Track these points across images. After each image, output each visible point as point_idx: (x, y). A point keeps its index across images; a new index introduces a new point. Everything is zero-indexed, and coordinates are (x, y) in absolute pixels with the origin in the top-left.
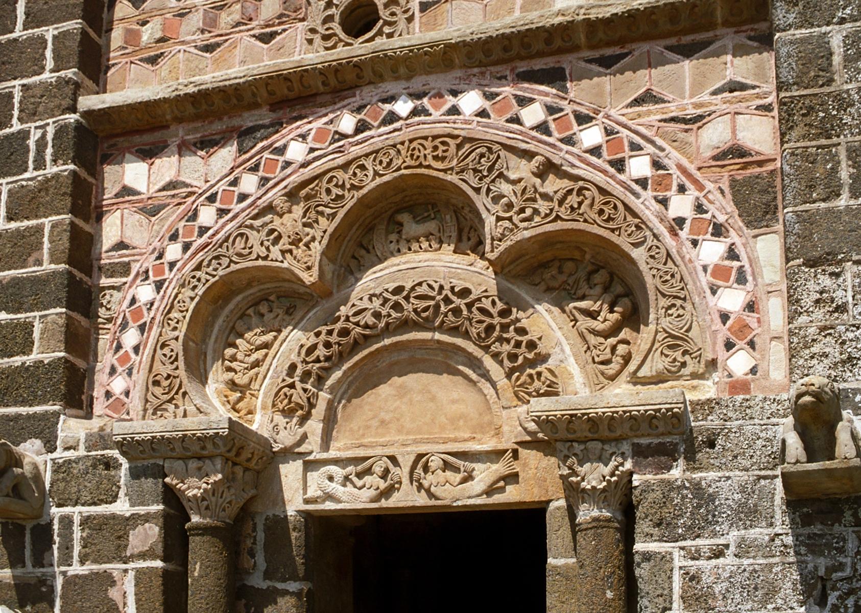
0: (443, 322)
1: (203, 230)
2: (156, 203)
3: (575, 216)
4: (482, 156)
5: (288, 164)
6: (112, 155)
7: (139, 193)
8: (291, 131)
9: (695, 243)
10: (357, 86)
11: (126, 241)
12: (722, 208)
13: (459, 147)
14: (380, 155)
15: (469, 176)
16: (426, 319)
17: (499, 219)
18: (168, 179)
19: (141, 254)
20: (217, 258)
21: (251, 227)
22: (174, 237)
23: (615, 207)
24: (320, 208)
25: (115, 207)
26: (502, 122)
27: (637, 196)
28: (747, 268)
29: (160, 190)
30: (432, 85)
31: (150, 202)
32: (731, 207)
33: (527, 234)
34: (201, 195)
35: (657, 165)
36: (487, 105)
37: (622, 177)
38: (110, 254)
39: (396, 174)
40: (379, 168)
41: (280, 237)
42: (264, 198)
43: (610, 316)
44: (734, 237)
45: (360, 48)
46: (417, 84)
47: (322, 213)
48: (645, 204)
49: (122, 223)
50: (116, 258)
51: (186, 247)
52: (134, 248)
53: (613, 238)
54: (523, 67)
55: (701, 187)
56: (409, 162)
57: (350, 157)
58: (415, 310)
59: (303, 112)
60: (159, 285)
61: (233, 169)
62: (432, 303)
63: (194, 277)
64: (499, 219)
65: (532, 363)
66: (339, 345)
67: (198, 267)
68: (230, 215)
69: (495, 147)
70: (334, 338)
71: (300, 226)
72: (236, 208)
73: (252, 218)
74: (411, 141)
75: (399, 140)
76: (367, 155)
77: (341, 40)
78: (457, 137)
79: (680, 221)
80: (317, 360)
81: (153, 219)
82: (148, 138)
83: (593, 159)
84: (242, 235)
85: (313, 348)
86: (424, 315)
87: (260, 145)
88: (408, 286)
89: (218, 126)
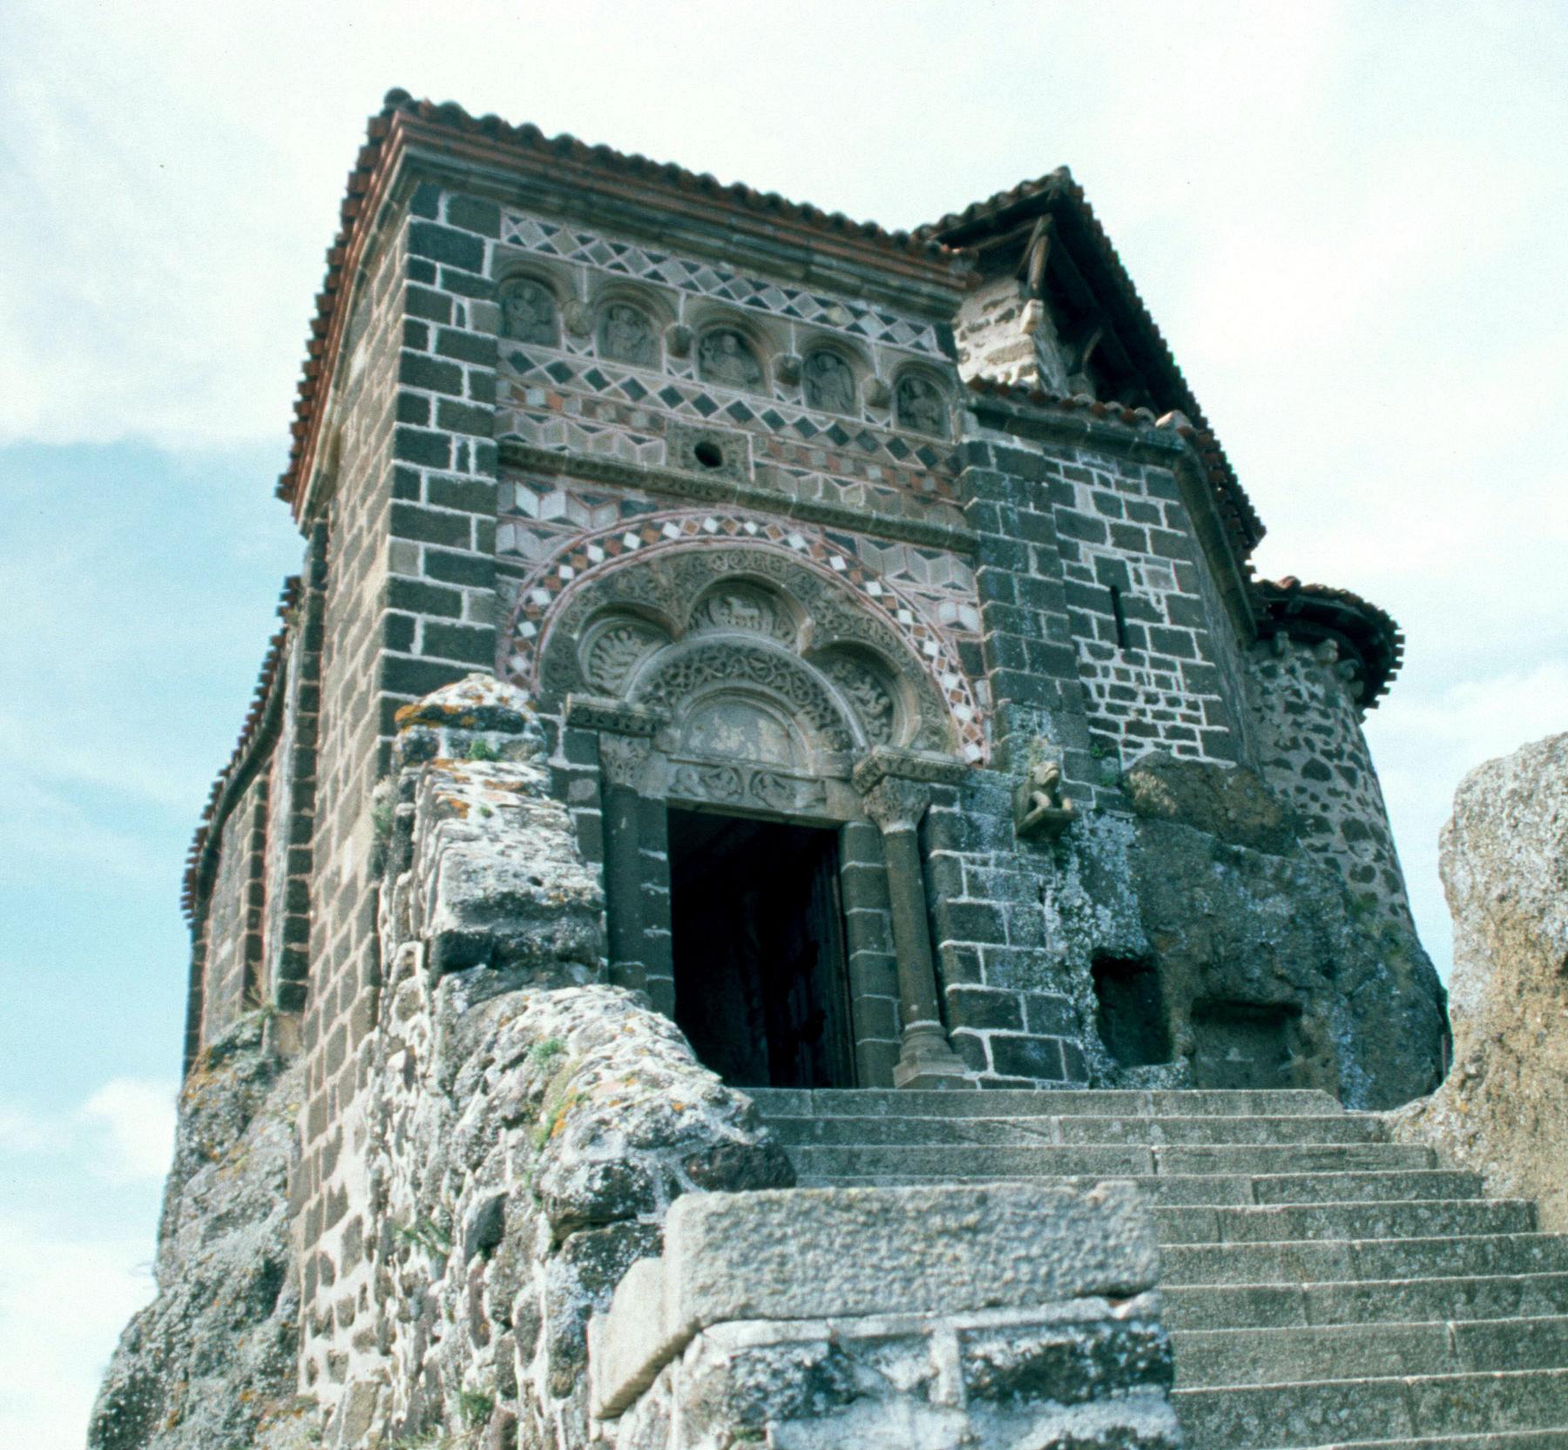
12: (954, 657)
22: (564, 559)
35: (915, 619)
46: (760, 515)
48: (909, 641)
54: (829, 529)
82: (540, 478)
89: (604, 490)
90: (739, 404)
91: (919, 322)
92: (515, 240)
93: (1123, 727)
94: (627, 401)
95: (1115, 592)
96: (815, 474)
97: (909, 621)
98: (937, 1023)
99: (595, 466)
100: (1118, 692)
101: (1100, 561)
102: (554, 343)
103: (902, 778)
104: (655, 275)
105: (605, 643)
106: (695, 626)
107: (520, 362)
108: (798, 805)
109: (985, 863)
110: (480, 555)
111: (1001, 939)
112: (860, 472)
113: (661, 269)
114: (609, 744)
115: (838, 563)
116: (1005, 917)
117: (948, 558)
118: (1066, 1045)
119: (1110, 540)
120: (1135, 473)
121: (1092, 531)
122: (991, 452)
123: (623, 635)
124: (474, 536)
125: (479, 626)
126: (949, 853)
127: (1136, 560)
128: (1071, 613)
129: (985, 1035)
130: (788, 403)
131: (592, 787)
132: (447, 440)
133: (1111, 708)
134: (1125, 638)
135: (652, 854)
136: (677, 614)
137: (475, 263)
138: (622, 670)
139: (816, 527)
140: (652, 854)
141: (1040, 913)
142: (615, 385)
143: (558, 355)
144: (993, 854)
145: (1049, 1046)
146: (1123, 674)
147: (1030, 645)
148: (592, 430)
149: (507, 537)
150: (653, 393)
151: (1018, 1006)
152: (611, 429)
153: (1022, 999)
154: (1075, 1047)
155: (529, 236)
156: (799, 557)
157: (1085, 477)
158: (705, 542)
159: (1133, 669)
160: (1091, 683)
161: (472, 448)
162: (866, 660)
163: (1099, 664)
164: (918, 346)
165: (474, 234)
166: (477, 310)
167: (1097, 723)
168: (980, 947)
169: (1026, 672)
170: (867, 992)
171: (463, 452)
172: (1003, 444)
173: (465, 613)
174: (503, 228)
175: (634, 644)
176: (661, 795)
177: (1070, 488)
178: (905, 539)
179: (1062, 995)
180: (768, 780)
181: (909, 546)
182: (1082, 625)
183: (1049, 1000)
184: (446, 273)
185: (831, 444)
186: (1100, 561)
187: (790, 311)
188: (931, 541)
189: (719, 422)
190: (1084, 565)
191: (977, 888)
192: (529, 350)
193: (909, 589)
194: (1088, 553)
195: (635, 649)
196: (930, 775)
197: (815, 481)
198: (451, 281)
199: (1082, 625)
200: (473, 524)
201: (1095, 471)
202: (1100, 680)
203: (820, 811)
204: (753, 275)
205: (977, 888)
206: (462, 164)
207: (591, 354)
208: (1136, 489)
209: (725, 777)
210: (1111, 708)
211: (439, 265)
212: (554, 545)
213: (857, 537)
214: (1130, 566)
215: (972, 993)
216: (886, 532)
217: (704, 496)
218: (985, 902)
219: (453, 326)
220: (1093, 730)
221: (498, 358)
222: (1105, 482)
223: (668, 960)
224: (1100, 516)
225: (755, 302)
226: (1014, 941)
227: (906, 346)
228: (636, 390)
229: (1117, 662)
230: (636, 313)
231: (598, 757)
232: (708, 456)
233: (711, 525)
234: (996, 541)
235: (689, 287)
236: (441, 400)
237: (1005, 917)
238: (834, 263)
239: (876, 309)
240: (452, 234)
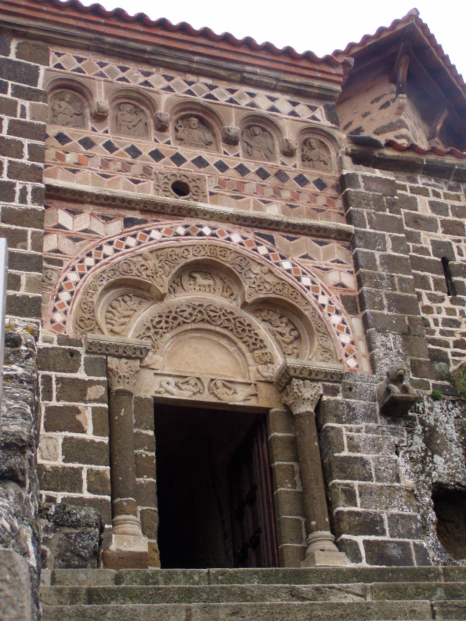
0: (221, 323)
1: (105, 256)
2: (78, 236)
3: (281, 293)
4: (241, 260)
5: (151, 239)
6: (50, 207)
7: (68, 230)
8: (153, 226)
9: (330, 315)
10: (185, 216)
11: (60, 250)
12: (338, 305)
13: (231, 253)
14: (196, 247)
15: (237, 266)
16: (214, 321)
17: (250, 287)
18: (85, 228)
19: (69, 258)
20: (112, 270)
21: (131, 261)
22: (89, 255)
23: (297, 294)
24: (167, 262)
25: (53, 232)
26: (250, 249)
27: (306, 292)
28: (350, 328)
29: (80, 231)
30: (219, 226)
31: (74, 235)
32: (341, 305)
33: (262, 296)
34: (104, 240)
35: (313, 282)
36: (243, 241)
37: (300, 283)
38: (51, 253)
39: (203, 257)
40: (195, 253)
41: (147, 269)
42: (139, 250)
43: (290, 337)
44: (343, 316)
45: (181, 201)
46: (213, 224)
47: (167, 264)
48: (309, 295)
49: (58, 240)
50: (54, 256)
51: (97, 261)
52: (65, 254)
53: (297, 305)
54: (257, 231)
55: (330, 295)
56: (209, 254)
57: (183, 245)
58: (209, 316)
59: (159, 219)
60: (82, 276)
61: (121, 234)
62: (217, 314)
63: (101, 276)
64: (250, 287)
65: (261, 347)
66: (173, 323)
67: (104, 272)
68: (120, 253)
69: (247, 259)
70: (170, 320)
71: (158, 268)
72: (124, 251)
73: (131, 257)
74: (210, 246)
75: (204, 244)
76: (190, 246)
77: (172, 194)
78: (230, 250)
79: (323, 306)
80: (162, 328)
81: (76, 243)
82: (72, 206)
83: (288, 274)
84: (126, 263)
85: (160, 322)
86: (213, 319)
87: (136, 227)
88: (206, 305)
90: (200, 157)
91: (313, 104)
92: (59, 66)
93: (451, 344)
94: (129, 159)
95: (445, 261)
96: (248, 197)
97: (309, 284)
98: (328, 533)
99: (107, 198)
100: (446, 322)
101: (433, 242)
102: (83, 125)
103: (303, 379)
104: (146, 83)
105: (115, 304)
106: (172, 290)
107: (62, 138)
108: (239, 398)
109: (358, 431)
110: (33, 252)
111: (370, 478)
112: (277, 193)
113: (150, 79)
114: (113, 363)
115: (263, 250)
116: (373, 464)
117: (334, 245)
118: (415, 545)
119: (440, 230)
120: (458, 189)
121: (430, 225)
122: (360, 179)
123: (127, 298)
124: (29, 241)
125: (31, 295)
126: (335, 425)
127: (459, 241)
128: (414, 275)
129: (359, 539)
130: (231, 155)
131: (102, 390)
132: (14, 185)
133: (442, 333)
134: (452, 289)
135: (144, 432)
136: (162, 283)
137: (34, 80)
138: (127, 320)
139: (249, 229)
140: (144, 432)
141: (396, 461)
142: (121, 149)
143: (86, 133)
144: (363, 425)
145: (404, 546)
146: (450, 311)
147: (387, 296)
148: (106, 177)
149: (51, 242)
150: (145, 154)
151: (382, 521)
152: (118, 175)
153: (385, 517)
154: (422, 546)
155: (67, 63)
156: (238, 248)
157: (423, 192)
158: (177, 240)
159: (458, 308)
160: (430, 318)
161: (29, 189)
162: (281, 308)
163: (434, 306)
164: (314, 118)
165: (33, 64)
166: (33, 108)
167: (434, 342)
168: (356, 483)
169: (385, 312)
170: (288, 515)
171: (24, 191)
172: (368, 174)
173: (23, 287)
174: (51, 58)
175: (133, 303)
176: (149, 396)
177: (415, 199)
178: (305, 234)
179: (412, 513)
180: (219, 384)
181: (309, 239)
182: (423, 283)
183: (402, 517)
184: (15, 88)
185: (258, 179)
186: (433, 242)
187: (231, 101)
188: (321, 234)
189: (188, 169)
190: (424, 246)
191: (353, 447)
192: (67, 131)
193: (308, 264)
194: (426, 239)
195: (135, 307)
196: (321, 377)
197: (248, 202)
198: (17, 92)
199: (423, 283)
200: (29, 234)
201: (430, 189)
202: (435, 315)
203: (253, 402)
204: (210, 82)
205: (353, 447)
206: (24, 22)
207: (106, 132)
208: (458, 198)
209: (192, 382)
210: (442, 333)
211: (10, 83)
212: (82, 246)
213: (276, 235)
214: (454, 245)
215: (350, 513)
216: (294, 230)
217: (178, 212)
218: (359, 455)
219: (18, 118)
220: (430, 346)
221: (47, 136)
222: (437, 195)
223: (155, 498)
224: (434, 215)
225: (209, 96)
226: (379, 479)
227: (305, 118)
228: (134, 152)
229: (447, 304)
230: (136, 106)
231: (108, 372)
232: (180, 189)
233: (181, 230)
234: (364, 233)
235: (167, 91)
236: (10, 162)
237: (373, 464)
238: (258, 70)
239: (288, 97)
240: (19, 63)
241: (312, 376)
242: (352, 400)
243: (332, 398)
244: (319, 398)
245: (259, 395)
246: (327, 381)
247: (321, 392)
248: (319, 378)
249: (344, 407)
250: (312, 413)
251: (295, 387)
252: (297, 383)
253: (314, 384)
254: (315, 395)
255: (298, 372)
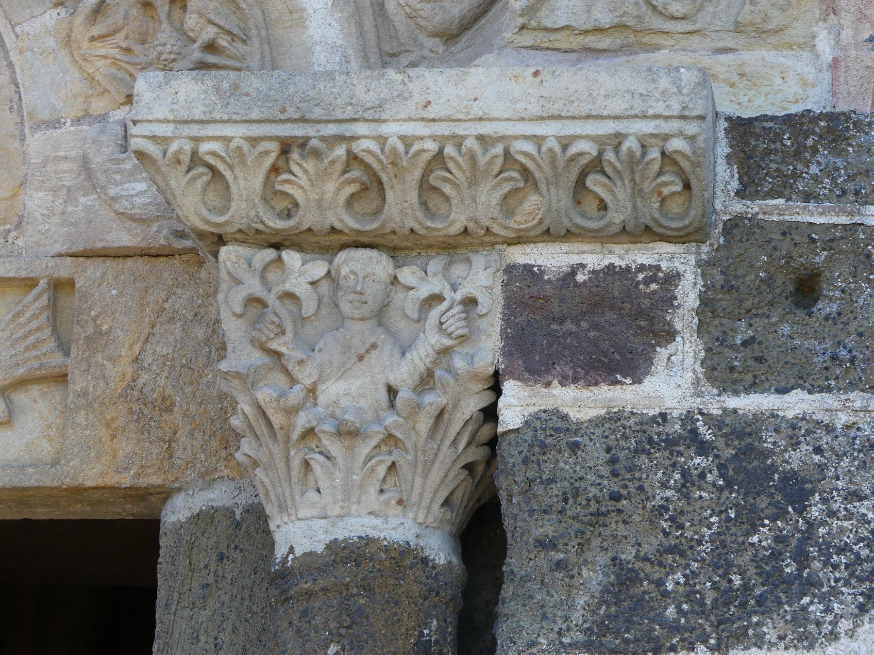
103: (328, 243)
241: (394, 214)
242: (796, 403)
243: (581, 402)
244: (480, 401)
245: (79, 382)
246: (548, 235)
247: (489, 350)
248: (458, 220)
249: (689, 481)
250: (404, 558)
251: (234, 329)
252: (253, 286)
253: (420, 280)
254: (426, 381)
255: (246, 184)
